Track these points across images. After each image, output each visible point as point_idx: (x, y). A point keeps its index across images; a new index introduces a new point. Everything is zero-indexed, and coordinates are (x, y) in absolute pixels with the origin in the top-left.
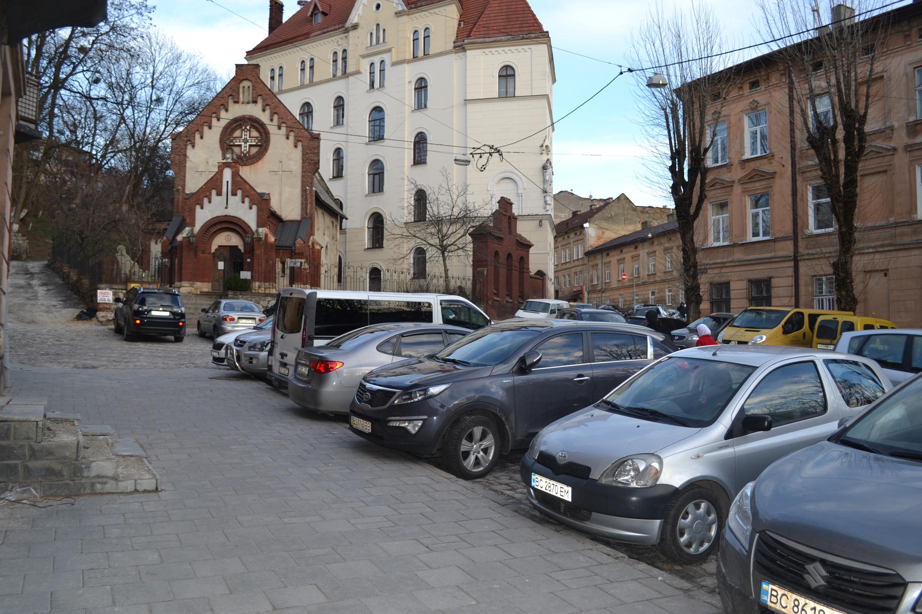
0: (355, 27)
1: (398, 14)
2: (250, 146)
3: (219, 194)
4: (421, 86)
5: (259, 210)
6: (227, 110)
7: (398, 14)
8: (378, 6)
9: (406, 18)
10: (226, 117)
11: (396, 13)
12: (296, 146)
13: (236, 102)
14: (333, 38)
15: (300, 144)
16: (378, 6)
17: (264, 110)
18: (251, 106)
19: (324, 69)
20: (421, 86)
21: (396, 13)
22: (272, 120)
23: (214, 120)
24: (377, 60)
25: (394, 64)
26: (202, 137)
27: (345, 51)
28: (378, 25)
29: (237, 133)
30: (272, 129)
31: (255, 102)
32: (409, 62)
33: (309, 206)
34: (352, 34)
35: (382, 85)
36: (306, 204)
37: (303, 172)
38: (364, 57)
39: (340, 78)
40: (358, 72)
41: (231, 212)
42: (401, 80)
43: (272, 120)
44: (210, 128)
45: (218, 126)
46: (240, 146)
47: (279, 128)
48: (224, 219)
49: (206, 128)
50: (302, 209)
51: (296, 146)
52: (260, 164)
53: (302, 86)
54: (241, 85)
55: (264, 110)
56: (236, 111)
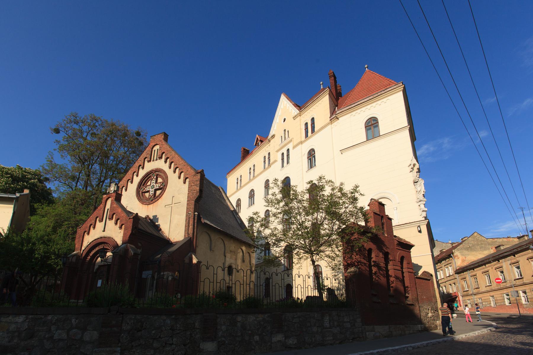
0: (273, 136)
1: (295, 118)
2: (156, 190)
3: (101, 221)
4: (311, 154)
5: (125, 229)
6: (143, 168)
7: (295, 118)
8: (285, 120)
9: (298, 119)
10: (142, 173)
11: (293, 118)
12: (185, 183)
13: (149, 161)
14: (263, 149)
15: (188, 180)
16: (285, 120)
17: (166, 162)
18: (158, 161)
19: (260, 167)
20: (311, 154)
21: (293, 118)
22: (170, 167)
23: (135, 177)
24: (285, 151)
25: (294, 147)
26: (126, 190)
27: (269, 154)
28: (285, 130)
29: (149, 183)
30: (169, 172)
31: (161, 158)
32: (301, 143)
33: (191, 227)
34: (272, 141)
35: (288, 163)
36: (189, 226)
37: (188, 201)
38: (278, 151)
39: (268, 168)
40: (275, 161)
41: (107, 234)
42: (299, 156)
43: (170, 167)
44: (132, 182)
45: (137, 180)
46: (148, 192)
47: (175, 172)
48: (100, 241)
49: (129, 183)
50: (185, 231)
51: (185, 183)
52: (160, 200)
53: (250, 180)
54: (154, 149)
55: (166, 162)
56: (149, 166)
